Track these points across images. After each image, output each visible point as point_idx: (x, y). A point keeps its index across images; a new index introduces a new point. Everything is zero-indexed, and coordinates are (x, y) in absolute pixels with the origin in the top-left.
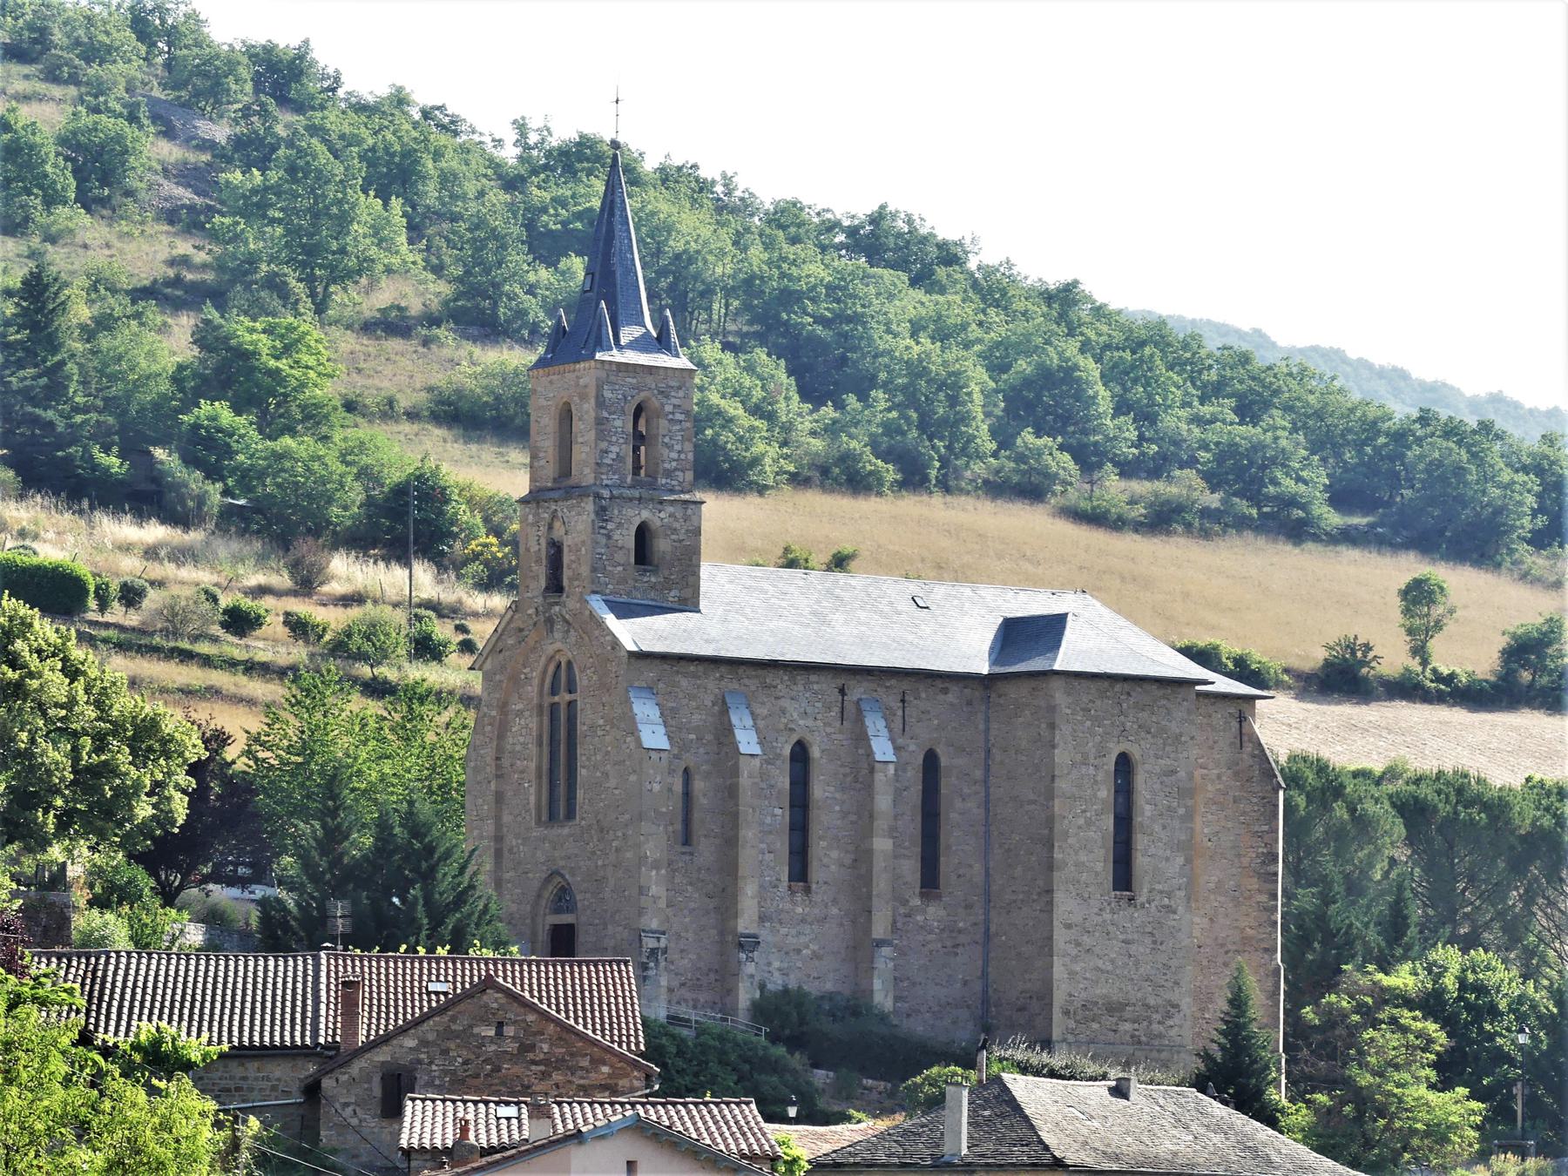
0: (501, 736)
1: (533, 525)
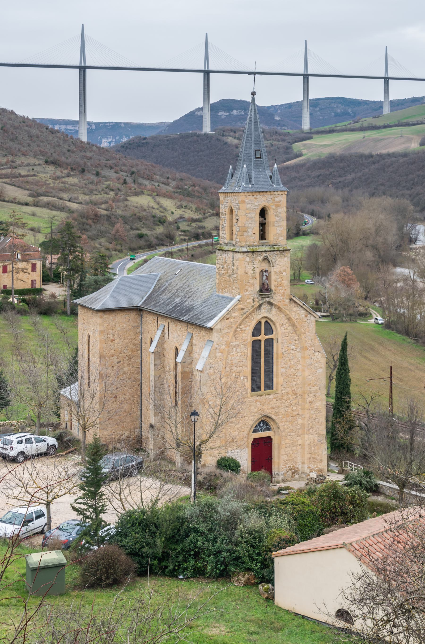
1: (250, 262)
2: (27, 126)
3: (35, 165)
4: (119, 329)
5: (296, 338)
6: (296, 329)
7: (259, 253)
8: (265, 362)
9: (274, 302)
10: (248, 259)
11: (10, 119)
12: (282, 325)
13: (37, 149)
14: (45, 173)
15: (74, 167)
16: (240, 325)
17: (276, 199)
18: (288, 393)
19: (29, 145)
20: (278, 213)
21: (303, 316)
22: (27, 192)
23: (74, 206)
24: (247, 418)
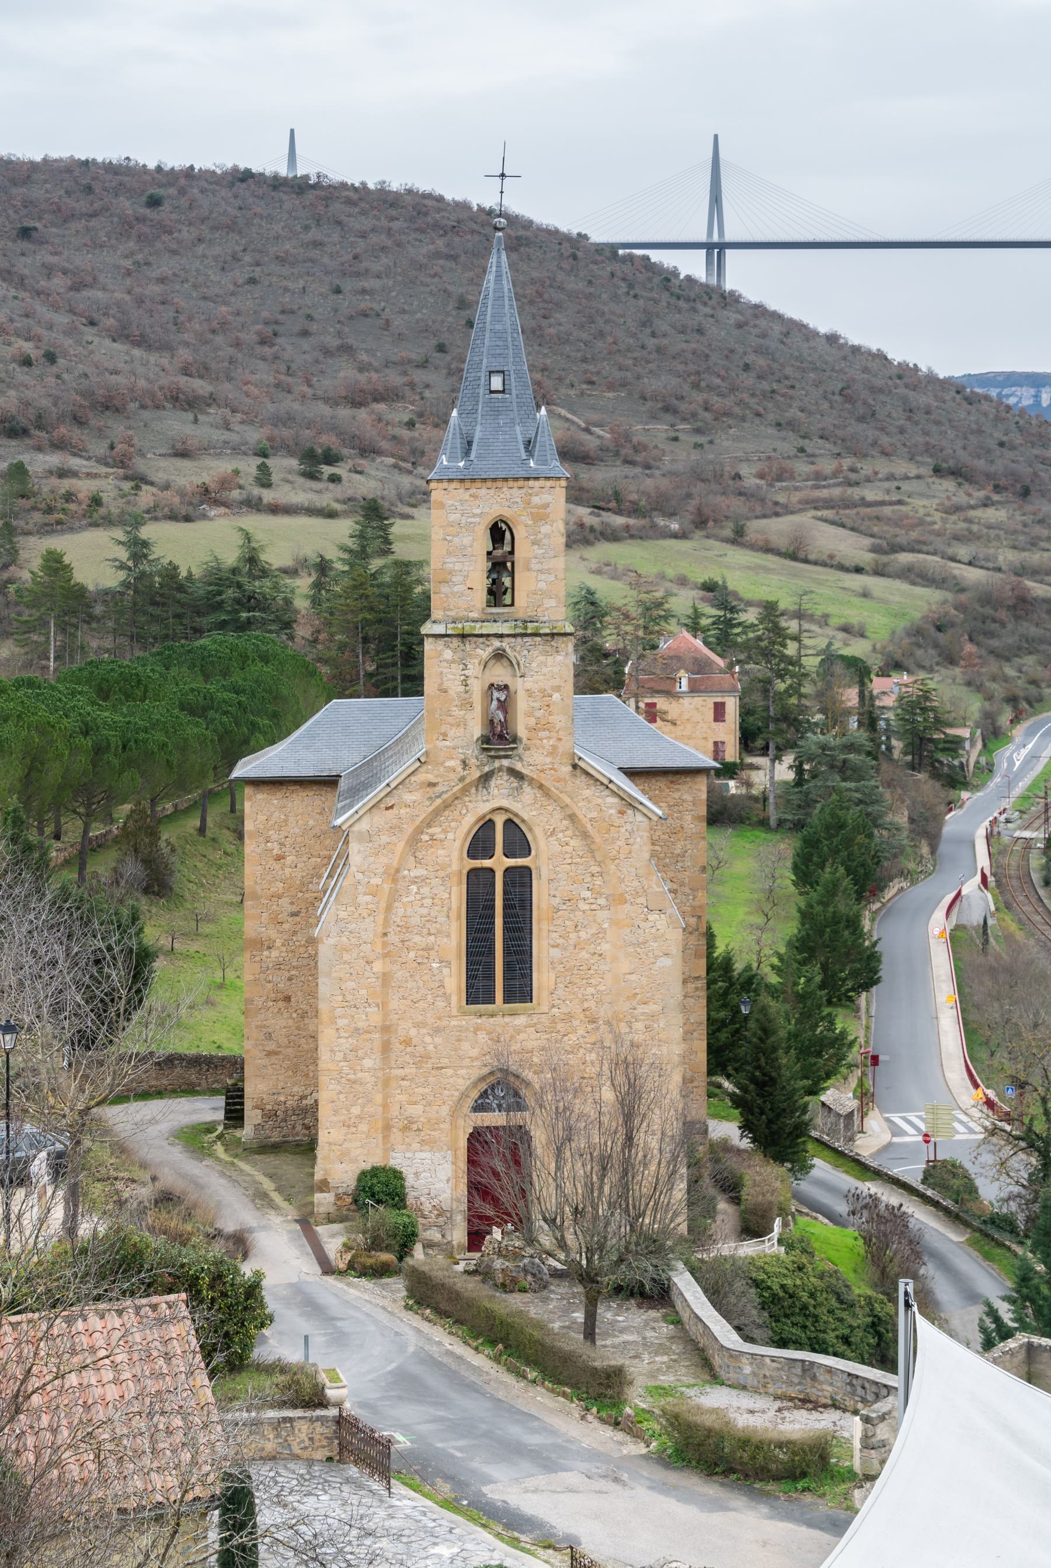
0: (389, 909)
1: (453, 662)
2: (907, 386)
3: (907, 478)
4: (297, 830)
5: (595, 869)
6: (593, 847)
7: (481, 640)
8: (506, 929)
9: (524, 771)
10: (448, 654)
11: (865, 370)
12: (552, 834)
13: (920, 439)
14: (928, 497)
15: (1003, 482)
16: (429, 826)
17: (536, 500)
18: (569, 1017)
19: (902, 431)
20: (540, 536)
21: (613, 811)
22: (868, 541)
23: (973, 575)
24: (450, 1072)
